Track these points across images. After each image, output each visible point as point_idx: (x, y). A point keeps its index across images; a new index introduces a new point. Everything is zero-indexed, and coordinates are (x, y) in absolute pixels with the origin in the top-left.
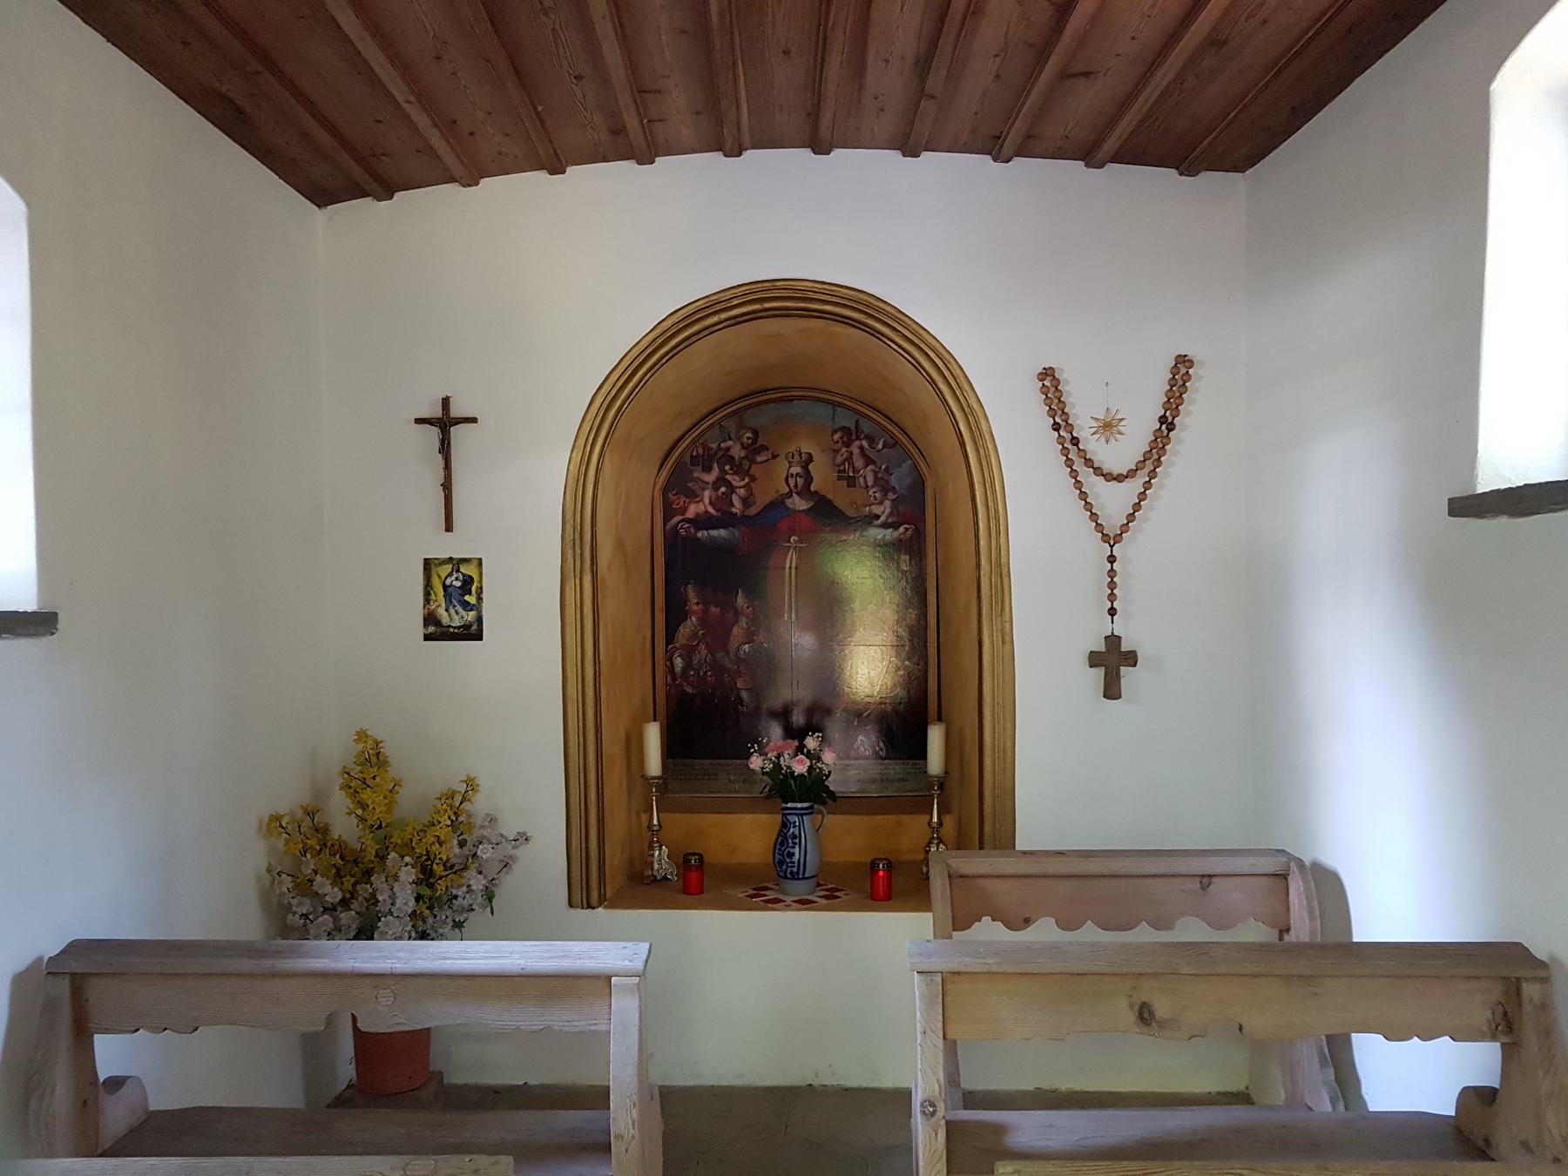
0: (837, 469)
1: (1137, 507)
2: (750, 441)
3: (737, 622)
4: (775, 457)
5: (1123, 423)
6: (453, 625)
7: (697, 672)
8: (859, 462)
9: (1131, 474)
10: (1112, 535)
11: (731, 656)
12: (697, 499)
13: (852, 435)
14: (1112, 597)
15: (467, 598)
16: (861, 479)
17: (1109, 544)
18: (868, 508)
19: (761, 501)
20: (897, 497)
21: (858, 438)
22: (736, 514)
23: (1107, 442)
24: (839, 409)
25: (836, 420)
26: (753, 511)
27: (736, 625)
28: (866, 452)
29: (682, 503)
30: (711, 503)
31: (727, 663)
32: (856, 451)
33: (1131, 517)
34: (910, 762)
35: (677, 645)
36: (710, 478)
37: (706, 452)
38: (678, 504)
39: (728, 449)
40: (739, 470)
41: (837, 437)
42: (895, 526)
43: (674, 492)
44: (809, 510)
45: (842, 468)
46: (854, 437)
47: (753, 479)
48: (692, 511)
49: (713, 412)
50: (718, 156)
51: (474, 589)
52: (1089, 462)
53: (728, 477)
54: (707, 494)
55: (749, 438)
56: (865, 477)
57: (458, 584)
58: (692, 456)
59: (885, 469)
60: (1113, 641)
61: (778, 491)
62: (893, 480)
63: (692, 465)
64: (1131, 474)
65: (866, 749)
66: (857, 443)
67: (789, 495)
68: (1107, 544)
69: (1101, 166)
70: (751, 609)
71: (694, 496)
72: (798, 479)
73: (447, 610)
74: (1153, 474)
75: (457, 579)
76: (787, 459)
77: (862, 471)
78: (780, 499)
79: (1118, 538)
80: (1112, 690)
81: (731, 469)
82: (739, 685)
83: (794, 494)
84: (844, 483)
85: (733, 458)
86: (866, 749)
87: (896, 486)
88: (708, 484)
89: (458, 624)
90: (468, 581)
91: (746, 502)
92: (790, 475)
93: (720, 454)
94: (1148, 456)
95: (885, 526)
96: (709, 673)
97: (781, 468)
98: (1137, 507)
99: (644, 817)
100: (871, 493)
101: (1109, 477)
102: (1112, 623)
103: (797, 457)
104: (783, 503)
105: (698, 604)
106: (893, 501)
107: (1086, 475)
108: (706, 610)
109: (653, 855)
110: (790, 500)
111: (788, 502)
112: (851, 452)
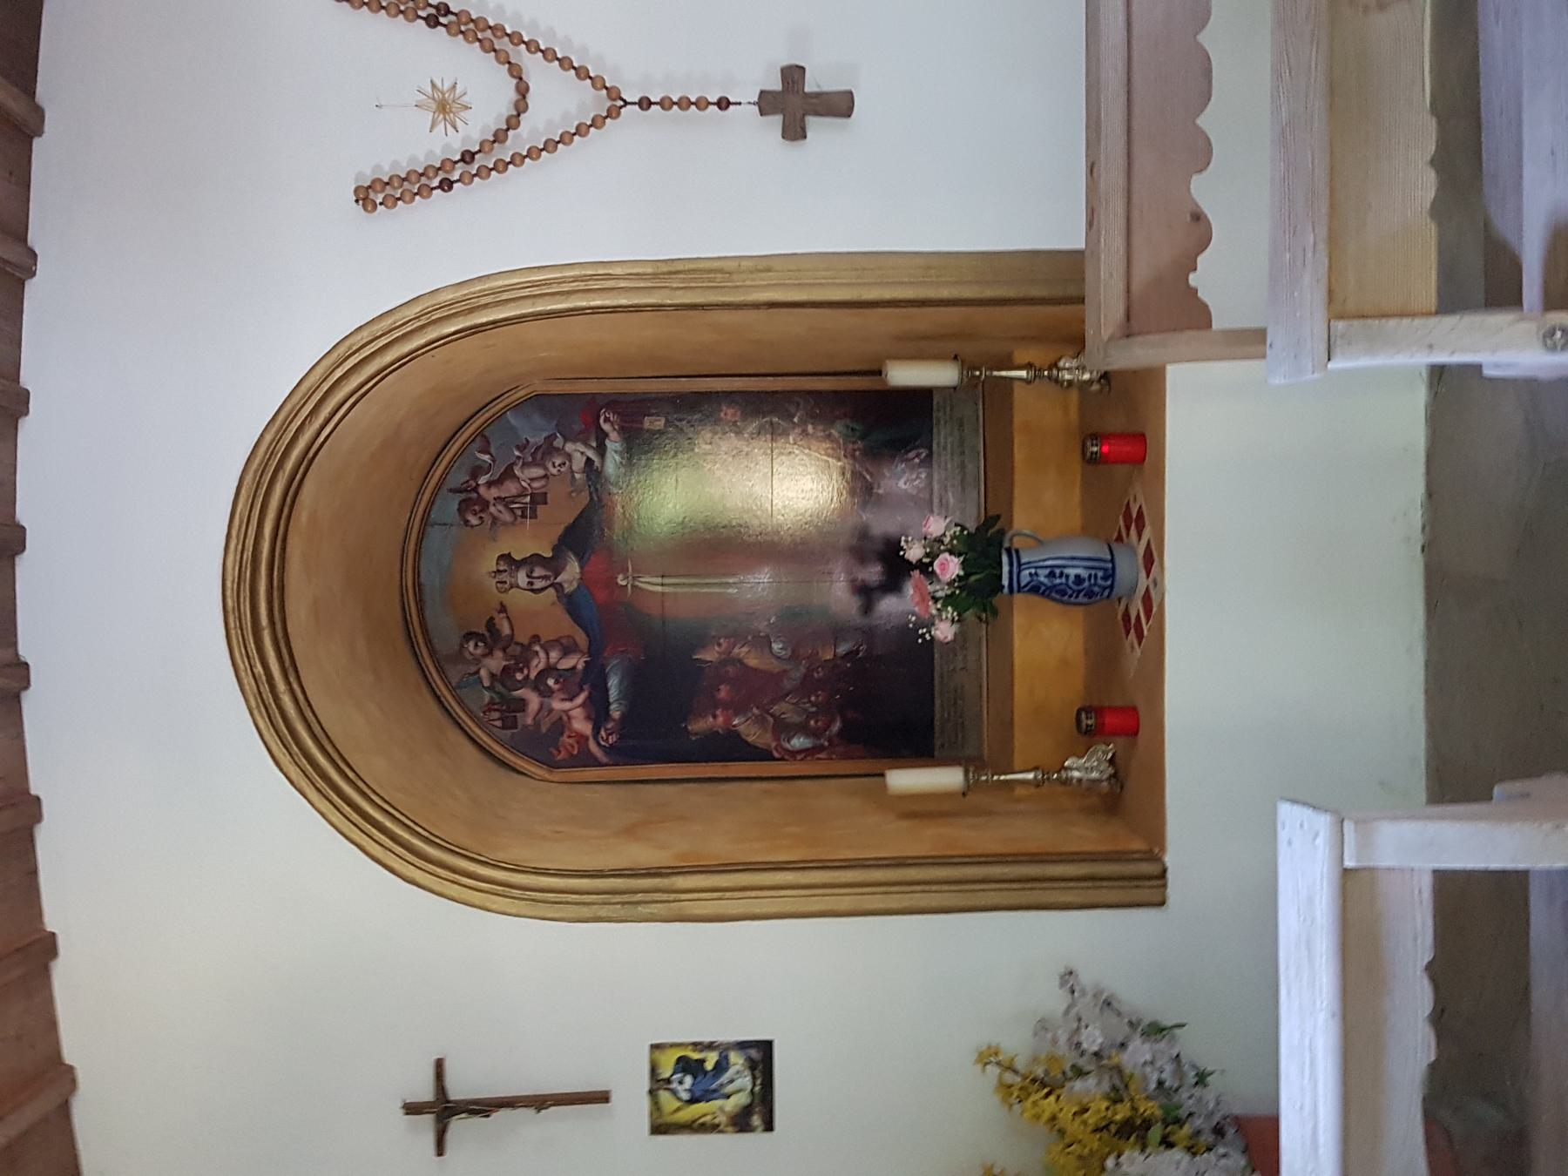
0: (519, 519)
1: (566, 63)
2: (480, 644)
3: (740, 661)
4: (503, 609)
5: (439, 84)
6: (750, 1087)
7: (810, 716)
8: (510, 488)
9: (516, 72)
10: (609, 104)
12: (565, 718)
13: (470, 499)
14: (702, 104)
15: (709, 1066)
16: (536, 485)
17: (621, 107)
18: (577, 476)
20: (561, 434)
21: (475, 489)
22: (585, 662)
23: (467, 108)
26: (582, 639)
27: (745, 661)
29: (571, 741)
30: (571, 700)
31: (798, 673)
32: (494, 492)
33: (582, 73)
34: (934, 414)
36: (534, 700)
37: (496, 707)
39: (492, 676)
40: (523, 660)
41: (474, 520)
42: (602, 436)
43: (555, 752)
44: (581, 558)
45: (519, 513)
46: (474, 495)
47: (536, 638)
48: (581, 725)
49: (438, 698)
50: (29, 701)
51: (696, 1056)
52: (499, 137)
53: (533, 675)
54: (558, 705)
55: (476, 645)
56: (532, 480)
57: (688, 1080)
58: (503, 728)
59: (521, 452)
60: (767, 103)
61: (553, 604)
62: (537, 439)
63: (515, 727)
64: (516, 72)
65: (917, 478)
66: (482, 490)
67: (558, 587)
68: (623, 110)
69: (39, 113)
71: (561, 724)
72: (535, 574)
73: (728, 1097)
74: (515, 38)
75: (681, 1083)
76: (506, 591)
77: (523, 483)
79: (613, 94)
80: (840, 105)
81: (521, 670)
83: (556, 581)
84: (540, 509)
85: (505, 669)
86: (917, 478)
87: (545, 434)
90: (686, 1066)
91: (566, 652)
92: (530, 587)
93: (499, 687)
94: (487, 44)
95: (601, 450)
97: (519, 599)
98: (566, 63)
99: (1020, 791)
100: (554, 471)
101: (521, 106)
102: (740, 104)
103: (504, 577)
104: (570, 596)
105: (715, 717)
106: (566, 440)
107: (520, 140)
108: (726, 706)
110: (566, 585)
111: (568, 589)
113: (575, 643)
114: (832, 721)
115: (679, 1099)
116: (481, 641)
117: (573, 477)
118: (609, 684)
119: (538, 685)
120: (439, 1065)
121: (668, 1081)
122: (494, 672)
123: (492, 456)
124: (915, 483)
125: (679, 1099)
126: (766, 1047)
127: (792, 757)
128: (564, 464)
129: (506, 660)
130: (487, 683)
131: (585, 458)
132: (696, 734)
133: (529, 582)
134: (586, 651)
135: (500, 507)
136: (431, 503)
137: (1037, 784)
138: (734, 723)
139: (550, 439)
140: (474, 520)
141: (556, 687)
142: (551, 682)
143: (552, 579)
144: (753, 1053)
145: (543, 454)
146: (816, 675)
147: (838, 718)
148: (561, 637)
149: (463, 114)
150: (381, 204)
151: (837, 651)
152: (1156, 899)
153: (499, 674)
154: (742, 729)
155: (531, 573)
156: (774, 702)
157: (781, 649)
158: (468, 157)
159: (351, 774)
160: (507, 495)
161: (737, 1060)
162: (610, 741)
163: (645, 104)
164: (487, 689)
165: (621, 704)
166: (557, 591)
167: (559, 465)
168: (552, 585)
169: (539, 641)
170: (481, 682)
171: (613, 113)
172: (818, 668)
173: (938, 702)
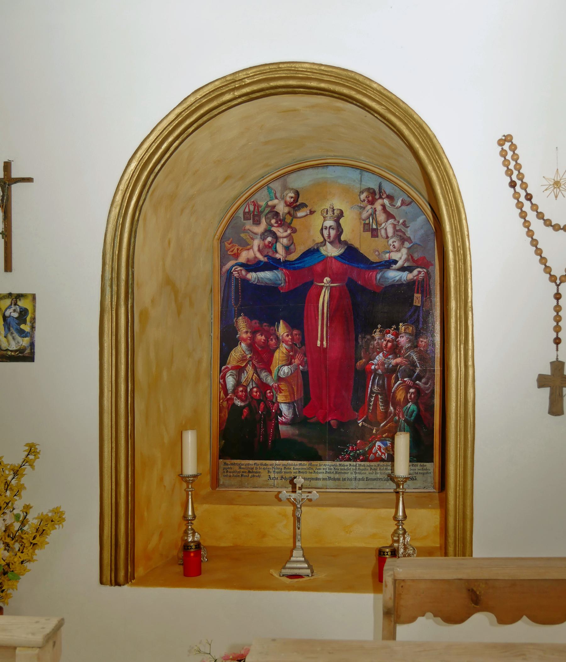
0: (363, 222)
2: (292, 200)
3: (278, 348)
4: (312, 212)
6: (11, 349)
7: (245, 387)
8: (381, 217)
11: (273, 376)
12: (249, 247)
13: (375, 194)
15: (22, 326)
16: (383, 232)
18: (387, 255)
19: (300, 250)
20: (412, 246)
21: (381, 197)
22: (280, 259)
24: (366, 174)
25: (363, 183)
26: (293, 257)
27: (278, 350)
28: (388, 209)
29: (235, 251)
30: (259, 250)
31: (270, 381)
32: (379, 208)
34: (419, 464)
35: (228, 366)
36: (260, 229)
37: (256, 208)
38: (232, 251)
39: (274, 207)
40: (282, 223)
41: (363, 196)
42: (409, 269)
43: (229, 242)
44: (341, 256)
45: (367, 222)
46: (377, 197)
47: (294, 231)
48: (244, 257)
51: (28, 319)
53: (274, 229)
54: (256, 243)
55: (292, 197)
56: (386, 229)
57: (16, 315)
58: (245, 213)
59: (402, 224)
61: (314, 240)
62: (409, 233)
63: (245, 219)
65: (382, 453)
66: (380, 201)
67: (324, 243)
70: (290, 337)
71: (246, 246)
72: (331, 231)
73: (6, 337)
75: (14, 311)
76: (322, 214)
77: (383, 225)
78: (316, 248)
81: (276, 222)
82: (280, 398)
83: (327, 242)
84: (369, 234)
85: (277, 214)
86: (382, 453)
87: (412, 238)
88: (256, 234)
89: (15, 348)
90: (23, 313)
91: (287, 249)
92: (324, 228)
93: (268, 210)
95: (402, 269)
96: (255, 389)
97: (317, 221)
100: (391, 242)
103: (330, 213)
104: (318, 250)
105: (247, 332)
106: (409, 249)
108: (253, 338)
110: (324, 248)
111: (323, 250)
112: (375, 208)
113: (291, 253)
114: (242, 401)
115: (6, 310)
116: (294, 200)
117: (387, 252)
118: (267, 272)
119: (269, 232)
120: (29, 180)
121: (16, 304)
122: (276, 207)
123: (400, 207)
124: (378, 451)
125: (6, 310)
126: (30, 358)
127: (221, 376)
128: (395, 248)
129: (283, 214)
130: (270, 203)
131: (397, 259)
132: (237, 322)
133: (327, 227)
134: (286, 259)
135: (370, 211)
136: (373, 173)
137: (185, 517)
138: (242, 344)
139: (409, 240)
140: (363, 196)
141: (266, 242)
142: (269, 239)
143: (328, 240)
144: (28, 351)
145: (401, 236)
146: (268, 391)
147: (243, 404)
148: (295, 245)
149: (553, 195)
150: (502, 149)
151: (282, 404)
152: (104, 580)
153: (275, 210)
154: (239, 348)
155: (332, 229)
156: (254, 366)
157: (284, 371)
158: (529, 197)
159: (191, 130)
160: (377, 215)
161: (25, 342)
162: (234, 273)
163: (558, 296)
164: (267, 204)
165: (256, 278)
166: (322, 243)
167: (394, 245)
168: (325, 240)
169: (292, 233)
170: (270, 200)
171: (553, 279)
172: (273, 393)
173: (251, 462)
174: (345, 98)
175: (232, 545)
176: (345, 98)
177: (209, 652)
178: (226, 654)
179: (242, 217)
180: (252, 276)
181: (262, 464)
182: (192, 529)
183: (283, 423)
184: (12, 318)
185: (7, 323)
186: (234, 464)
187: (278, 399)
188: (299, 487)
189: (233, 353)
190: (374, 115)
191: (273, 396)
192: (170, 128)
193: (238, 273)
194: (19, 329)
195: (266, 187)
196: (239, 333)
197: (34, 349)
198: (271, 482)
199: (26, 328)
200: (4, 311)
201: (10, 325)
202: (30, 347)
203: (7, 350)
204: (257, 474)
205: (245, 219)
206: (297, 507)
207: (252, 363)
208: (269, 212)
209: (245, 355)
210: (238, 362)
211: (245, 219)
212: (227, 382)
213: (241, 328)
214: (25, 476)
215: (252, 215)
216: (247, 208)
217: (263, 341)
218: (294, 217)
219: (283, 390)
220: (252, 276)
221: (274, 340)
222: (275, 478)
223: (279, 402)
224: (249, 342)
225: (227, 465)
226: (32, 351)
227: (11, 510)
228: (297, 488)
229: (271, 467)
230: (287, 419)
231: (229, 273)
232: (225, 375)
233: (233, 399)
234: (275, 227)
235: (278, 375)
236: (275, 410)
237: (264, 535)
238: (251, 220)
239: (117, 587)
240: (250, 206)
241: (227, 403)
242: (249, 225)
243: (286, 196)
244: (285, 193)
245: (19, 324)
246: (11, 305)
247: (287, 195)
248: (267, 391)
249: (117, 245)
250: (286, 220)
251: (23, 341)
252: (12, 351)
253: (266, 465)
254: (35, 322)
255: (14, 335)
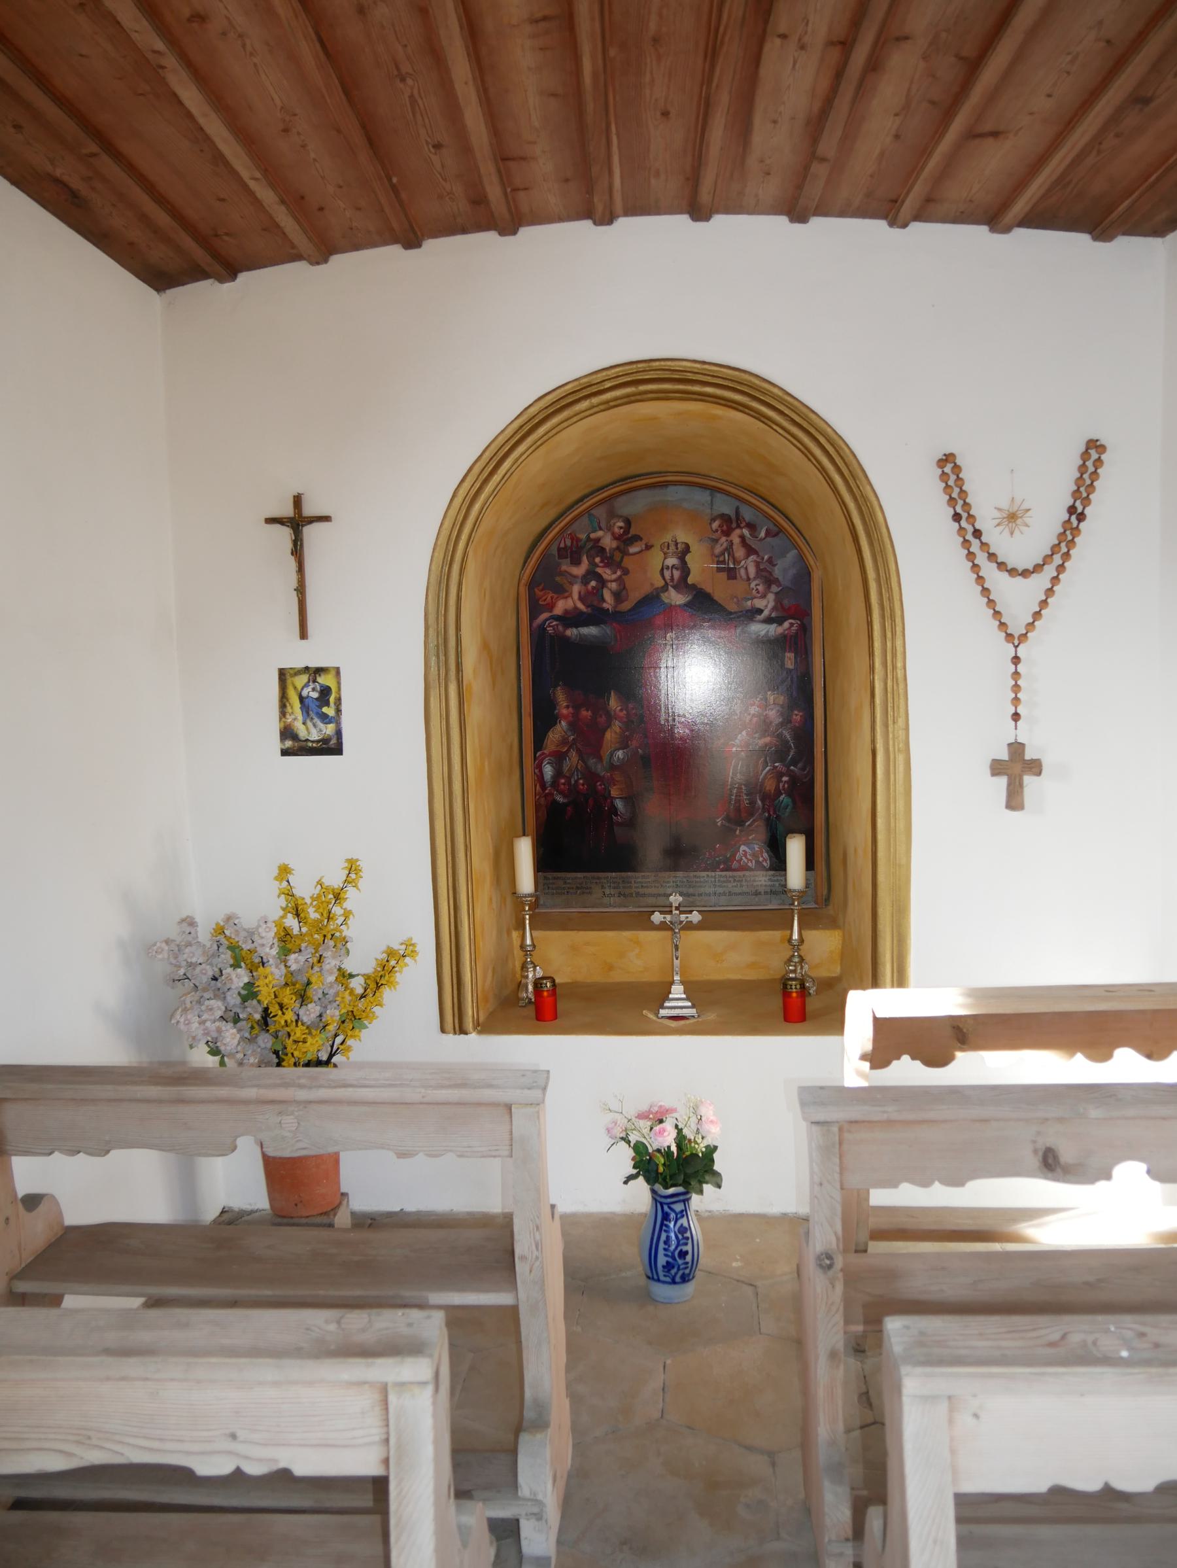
0: (716, 559)
1: (1044, 603)
2: (622, 531)
3: (609, 726)
4: (648, 547)
6: (310, 739)
7: (568, 779)
8: (740, 552)
9: (1038, 568)
11: (604, 762)
12: (567, 594)
13: (731, 523)
15: (325, 710)
16: (743, 572)
18: (749, 603)
19: (635, 596)
20: (781, 590)
21: (738, 526)
22: (608, 609)
24: (719, 495)
25: (714, 507)
26: (626, 606)
27: (609, 730)
28: (748, 541)
29: (549, 598)
30: (581, 599)
31: (600, 769)
32: (736, 540)
35: (545, 752)
36: (579, 571)
37: (575, 542)
38: (545, 600)
39: (598, 540)
40: (609, 562)
41: (715, 525)
42: (779, 621)
43: (541, 587)
44: (688, 605)
45: (721, 559)
46: (734, 525)
47: (626, 572)
48: (561, 607)
49: (581, 500)
51: (332, 699)
53: (599, 570)
54: (576, 589)
55: (621, 528)
56: (746, 568)
57: (315, 695)
58: (559, 549)
61: (652, 585)
62: (777, 572)
64: (1038, 568)
65: (748, 860)
66: (738, 532)
67: (665, 588)
70: (625, 712)
73: (304, 723)
75: (314, 690)
76: (662, 549)
78: (655, 593)
79: (1023, 637)
81: (602, 561)
82: (614, 793)
83: (670, 587)
84: (724, 575)
85: (603, 549)
86: (748, 860)
87: (780, 578)
88: (575, 577)
89: (317, 738)
90: (325, 692)
91: (618, 596)
92: (665, 567)
93: (590, 545)
95: (769, 620)
96: (581, 781)
98: (1044, 603)
99: (515, 935)
100: (753, 585)
103: (672, 548)
105: (567, 707)
106: (777, 594)
108: (576, 715)
109: (527, 977)
110: (666, 594)
111: (664, 597)
112: (731, 541)
113: (622, 602)
114: (565, 796)
115: (302, 689)
116: (624, 532)
117: (749, 599)
118: (591, 627)
119: (591, 574)
121: (315, 681)
122: (601, 541)
123: (764, 539)
124: (743, 858)
125: (302, 689)
126: (337, 750)
127: (537, 765)
128: (758, 592)
129: (610, 550)
130: (593, 536)
131: (762, 608)
132: (554, 693)
133: (668, 566)
134: (617, 610)
135: (725, 545)
136: (728, 494)
137: (523, 946)
138: (562, 722)
139: (777, 581)
140: (715, 525)
141: (589, 587)
142: (593, 583)
143: (671, 584)
144: (334, 741)
145: (766, 577)
146: (599, 783)
147: (565, 801)
148: (627, 590)
150: (943, 471)
151: (617, 800)
153: (600, 545)
154: (558, 727)
155: (676, 568)
156: (579, 751)
157: (618, 757)
158: (977, 533)
160: (734, 550)
161: (330, 729)
162: (548, 629)
163: (1016, 660)
164: (588, 536)
165: (577, 635)
166: (663, 587)
167: (757, 589)
168: (666, 584)
169: (624, 574)
170: (593, 532)
171: (1009, 637)
172: (604, 785)
173: (579, 875)
174: (734, 405)
175: (569, 981)
176: (734, 405)
177: (620, 1111)
178: (640, 1112)
179: (557, 555)
180: (571, 632)
181: (593, 878)
182: (532, 962)
183: (620, 824)
184: (311, 699)
185: (304, 705)
186: (558, 878)
187: (612, 792)
188: (676, 907)
189: (550, 734)
190: (772, 428)
191: (605, 789)
192: (507, 448)
193: (554, 629)
194: (320, 713)
195: (587, 515)
196: (558, 707)
197: (341, 739)
198: (606, 900)
199: (330, 711)
200: (299, 690)
201: (308, 709)
202: (335, 736)
203: (307, 740)
204: (588, 891)
205: (560, 557)
206: (675, 933)
207: (577, 747)
208: (591, 548)
209: (566, 736)
210: (557, 746)
211: (560, 557)
212: (544, 772)
213: (560, 702)
214: (348, 899)
215: (569, 551)
216: (563, 541)
217: (589, 718)
218: (625, 553)
219: (617, 781)
220: (571, 632)
221: (603, 717)
222: (610, 895)
223: (613, 797)
224: (571, 719)
225: (548, 879)
226: (340, 741)
227: (344, 943)
228: (674, 908)
229: (606, 881)
230: (625, 819)
231: (542, 628)
232: (542, 763)
233: (553, 794)
234: (600, 567)
235: (610, 761)
236: (608, 807)
237: (611, 968)
238: (567, 558)
239: (462, 1036)
240: (566, 540)
241: (546, 799)
242: (565, 566)
243: (613, 526)
244: (612, 521)
245: (321, 707)
246: (309, 682)
247: (614, 524)
248: (597, 782)
249: (443, 601)
250: (615, 557)
251: (326, 729)
252: (313, 742)
253: (599, 878)
254: (340, 704)
255: (314, 721)
